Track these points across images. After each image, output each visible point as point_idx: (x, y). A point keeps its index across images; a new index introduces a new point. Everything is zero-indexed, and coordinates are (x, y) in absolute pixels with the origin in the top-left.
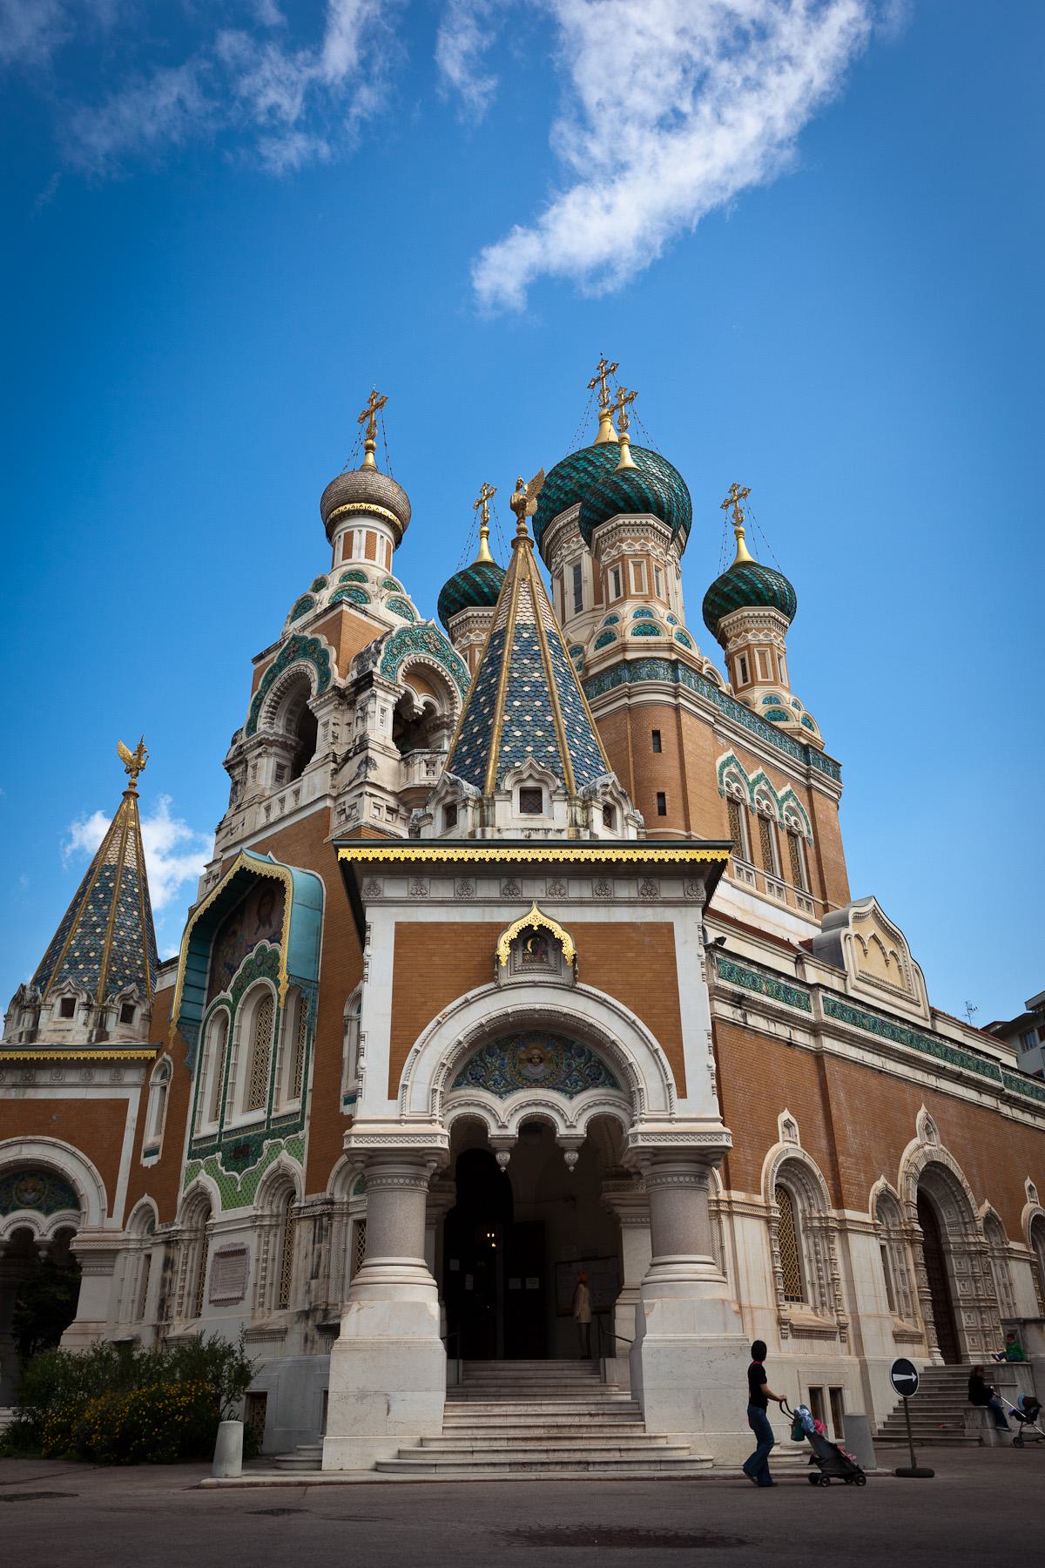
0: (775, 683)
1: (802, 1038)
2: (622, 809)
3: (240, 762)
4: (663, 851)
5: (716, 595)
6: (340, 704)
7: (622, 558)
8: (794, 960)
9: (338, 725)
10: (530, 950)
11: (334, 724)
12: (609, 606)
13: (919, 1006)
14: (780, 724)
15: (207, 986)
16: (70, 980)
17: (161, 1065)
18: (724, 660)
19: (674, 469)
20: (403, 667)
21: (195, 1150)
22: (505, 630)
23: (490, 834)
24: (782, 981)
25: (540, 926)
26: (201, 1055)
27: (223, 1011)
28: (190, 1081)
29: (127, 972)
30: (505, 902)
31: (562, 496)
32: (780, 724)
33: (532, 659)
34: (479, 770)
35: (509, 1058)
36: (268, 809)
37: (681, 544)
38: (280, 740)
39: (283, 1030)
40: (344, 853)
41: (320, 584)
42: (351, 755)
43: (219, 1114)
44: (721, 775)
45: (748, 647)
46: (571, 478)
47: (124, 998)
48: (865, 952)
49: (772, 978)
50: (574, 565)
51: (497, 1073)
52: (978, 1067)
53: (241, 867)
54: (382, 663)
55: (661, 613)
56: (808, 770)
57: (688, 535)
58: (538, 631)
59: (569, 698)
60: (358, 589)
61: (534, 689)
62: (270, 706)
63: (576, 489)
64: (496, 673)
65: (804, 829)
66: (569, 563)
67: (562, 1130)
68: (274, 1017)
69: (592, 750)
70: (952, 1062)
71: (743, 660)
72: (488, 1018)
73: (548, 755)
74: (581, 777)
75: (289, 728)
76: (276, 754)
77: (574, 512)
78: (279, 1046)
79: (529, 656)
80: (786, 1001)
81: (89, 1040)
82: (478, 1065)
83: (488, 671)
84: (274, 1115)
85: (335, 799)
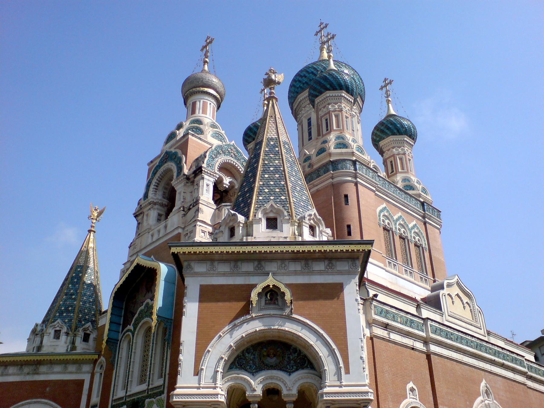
0: (407, 172)
1: (419, 345)
2: (319, 227)
3: (141, 213)
4: (337, 246)
5: (377, 130)
6: (187, 183)
7: (329, 113)
8: (416, 306)
9: (185, 193)
10: (269, 298)
11: (184, 192)
12: (323, 136)
13: (481, 329)
14: (411, 192)
15: (122, 323)
16: (59, 320)
17: (100, 363)
18: (382, 162)
19: (356, 71)
20: (217, 164)
21: (114, 405)
22: (262, 141)
23: (250, 239)
24: (409, 316)
25: (274, 285)
26: (118, 357)
27: (129, 335)
28: (113, 370)
29: (87, 317)
30: (256, 273)
31: (301, 85)
32: (411, 192)
33: (275, 154)
34: (247, 209)
35: (258, 355)
36: (152, 236)
37: (360, 107)
38: (160, 202)
39: (156, 344)
40: (174, 250)
41: (180, 127)
42: (191, 207)
43: (126, 387)
44: (380, 216)
45: (393, 155)
46: (305, 77)
47: (84, 330)
48: (453, 303)
49: (403, 315)
50: (309, 117)
51: (251, 362)
52: (514, 360)
53: (137, 263)
54: (207, 162)
55: (349, 137)
56: (424, 214)
57: (363, 103)
58: (278, 141)
59: (293, 173)
60: (197, 128)
61: (275, 169)
62: (155, 185)
63: (308, 82)
64: (257, 162)
65: (424, 243)
66: (305, 117)
67: (284, 392)
68: (152, 338)
69: (305, 198)
70: (499, 357)
71: (391, 162)
72: (246, 333)
73: (281, 200)
74: (298, 211)
75: (164, 196)
76: (157, 209)
77: (305, 94)
78: (154, 352)
79: (273, 153)
80: (411, 327)
81: (67, 350)
82: (241, 358)
83: (253, 161)
84: (151, 387)
85: (183, 229)
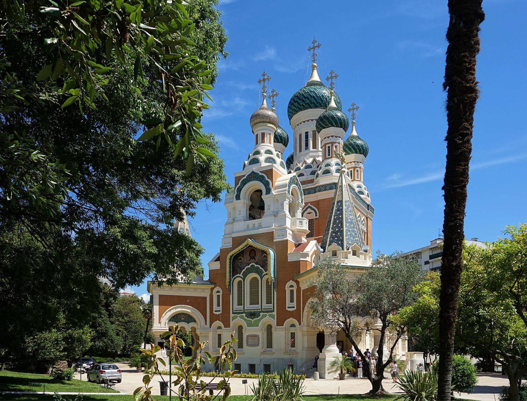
28: (230, 294)
31: (304, 104)
43: (240, 304)
46: (308, 99)
